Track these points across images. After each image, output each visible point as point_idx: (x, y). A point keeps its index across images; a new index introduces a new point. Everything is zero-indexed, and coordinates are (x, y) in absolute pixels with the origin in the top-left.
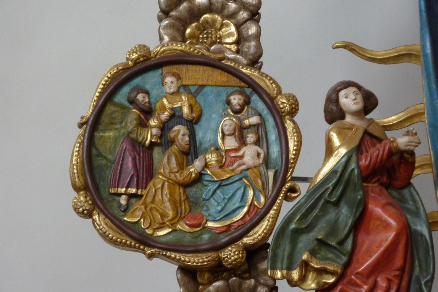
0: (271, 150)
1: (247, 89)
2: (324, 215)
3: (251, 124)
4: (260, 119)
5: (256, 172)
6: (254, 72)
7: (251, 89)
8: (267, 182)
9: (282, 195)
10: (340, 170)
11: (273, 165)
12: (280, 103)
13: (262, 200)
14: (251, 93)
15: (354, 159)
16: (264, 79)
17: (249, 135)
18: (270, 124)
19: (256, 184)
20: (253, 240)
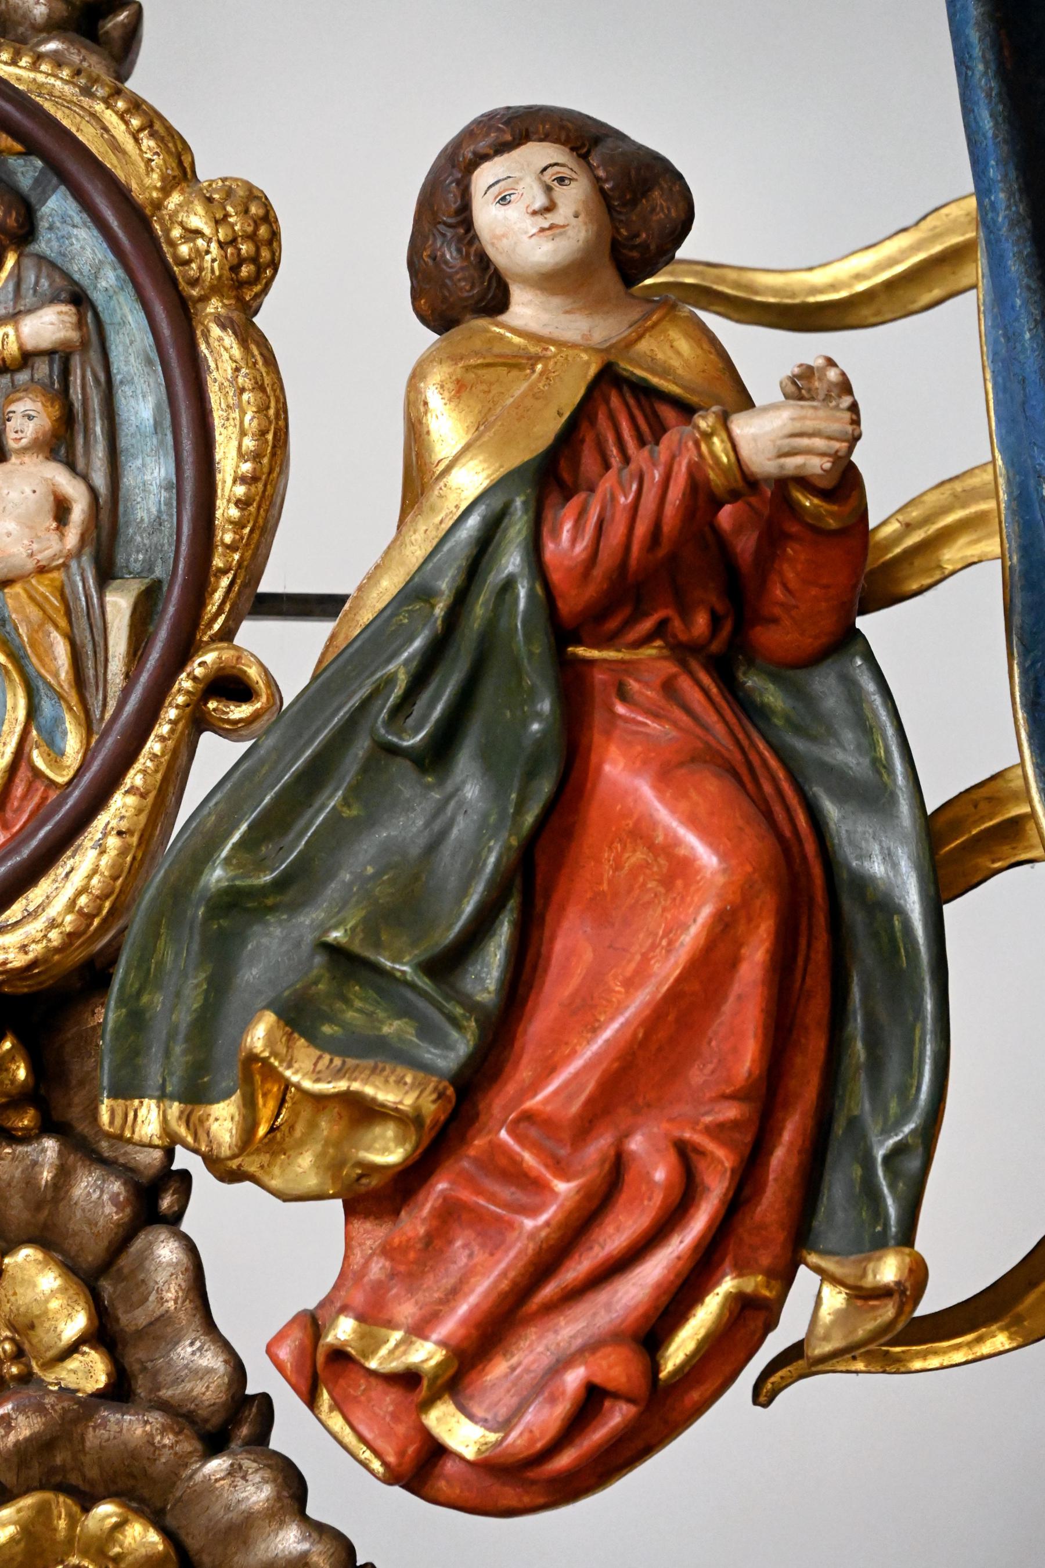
0: (129, 480)
1: (21, 161)
2: (369, 822)
3: (30, 345)
4: (74, 319)
5: (46, 598)
6: (48, 75)
7: (39, 164)
8: (100, 650)
9: (172, 713)
10: (445, 585)
11: (141, 557)
12: (176, 232)
13: (73, 744)
14: (37, 181)
15: (517, 529)
16: (99, 107)
17: (12, 408)
18: (131, 343)
19: (41, 660)
20: (24, 948)
